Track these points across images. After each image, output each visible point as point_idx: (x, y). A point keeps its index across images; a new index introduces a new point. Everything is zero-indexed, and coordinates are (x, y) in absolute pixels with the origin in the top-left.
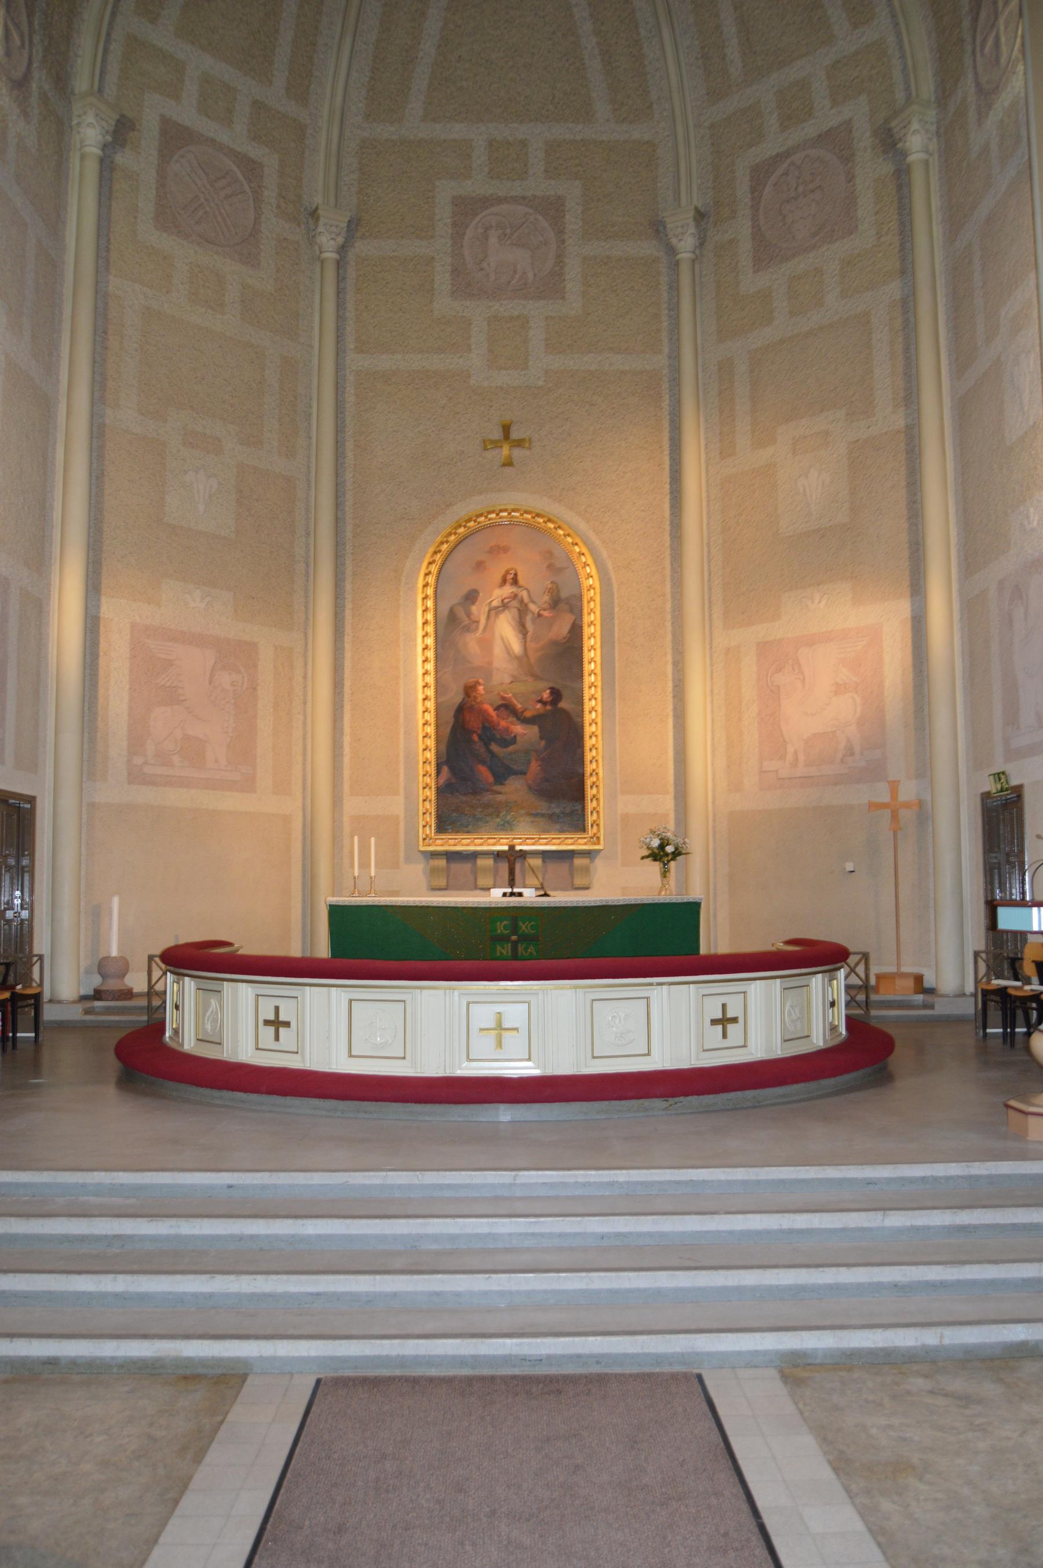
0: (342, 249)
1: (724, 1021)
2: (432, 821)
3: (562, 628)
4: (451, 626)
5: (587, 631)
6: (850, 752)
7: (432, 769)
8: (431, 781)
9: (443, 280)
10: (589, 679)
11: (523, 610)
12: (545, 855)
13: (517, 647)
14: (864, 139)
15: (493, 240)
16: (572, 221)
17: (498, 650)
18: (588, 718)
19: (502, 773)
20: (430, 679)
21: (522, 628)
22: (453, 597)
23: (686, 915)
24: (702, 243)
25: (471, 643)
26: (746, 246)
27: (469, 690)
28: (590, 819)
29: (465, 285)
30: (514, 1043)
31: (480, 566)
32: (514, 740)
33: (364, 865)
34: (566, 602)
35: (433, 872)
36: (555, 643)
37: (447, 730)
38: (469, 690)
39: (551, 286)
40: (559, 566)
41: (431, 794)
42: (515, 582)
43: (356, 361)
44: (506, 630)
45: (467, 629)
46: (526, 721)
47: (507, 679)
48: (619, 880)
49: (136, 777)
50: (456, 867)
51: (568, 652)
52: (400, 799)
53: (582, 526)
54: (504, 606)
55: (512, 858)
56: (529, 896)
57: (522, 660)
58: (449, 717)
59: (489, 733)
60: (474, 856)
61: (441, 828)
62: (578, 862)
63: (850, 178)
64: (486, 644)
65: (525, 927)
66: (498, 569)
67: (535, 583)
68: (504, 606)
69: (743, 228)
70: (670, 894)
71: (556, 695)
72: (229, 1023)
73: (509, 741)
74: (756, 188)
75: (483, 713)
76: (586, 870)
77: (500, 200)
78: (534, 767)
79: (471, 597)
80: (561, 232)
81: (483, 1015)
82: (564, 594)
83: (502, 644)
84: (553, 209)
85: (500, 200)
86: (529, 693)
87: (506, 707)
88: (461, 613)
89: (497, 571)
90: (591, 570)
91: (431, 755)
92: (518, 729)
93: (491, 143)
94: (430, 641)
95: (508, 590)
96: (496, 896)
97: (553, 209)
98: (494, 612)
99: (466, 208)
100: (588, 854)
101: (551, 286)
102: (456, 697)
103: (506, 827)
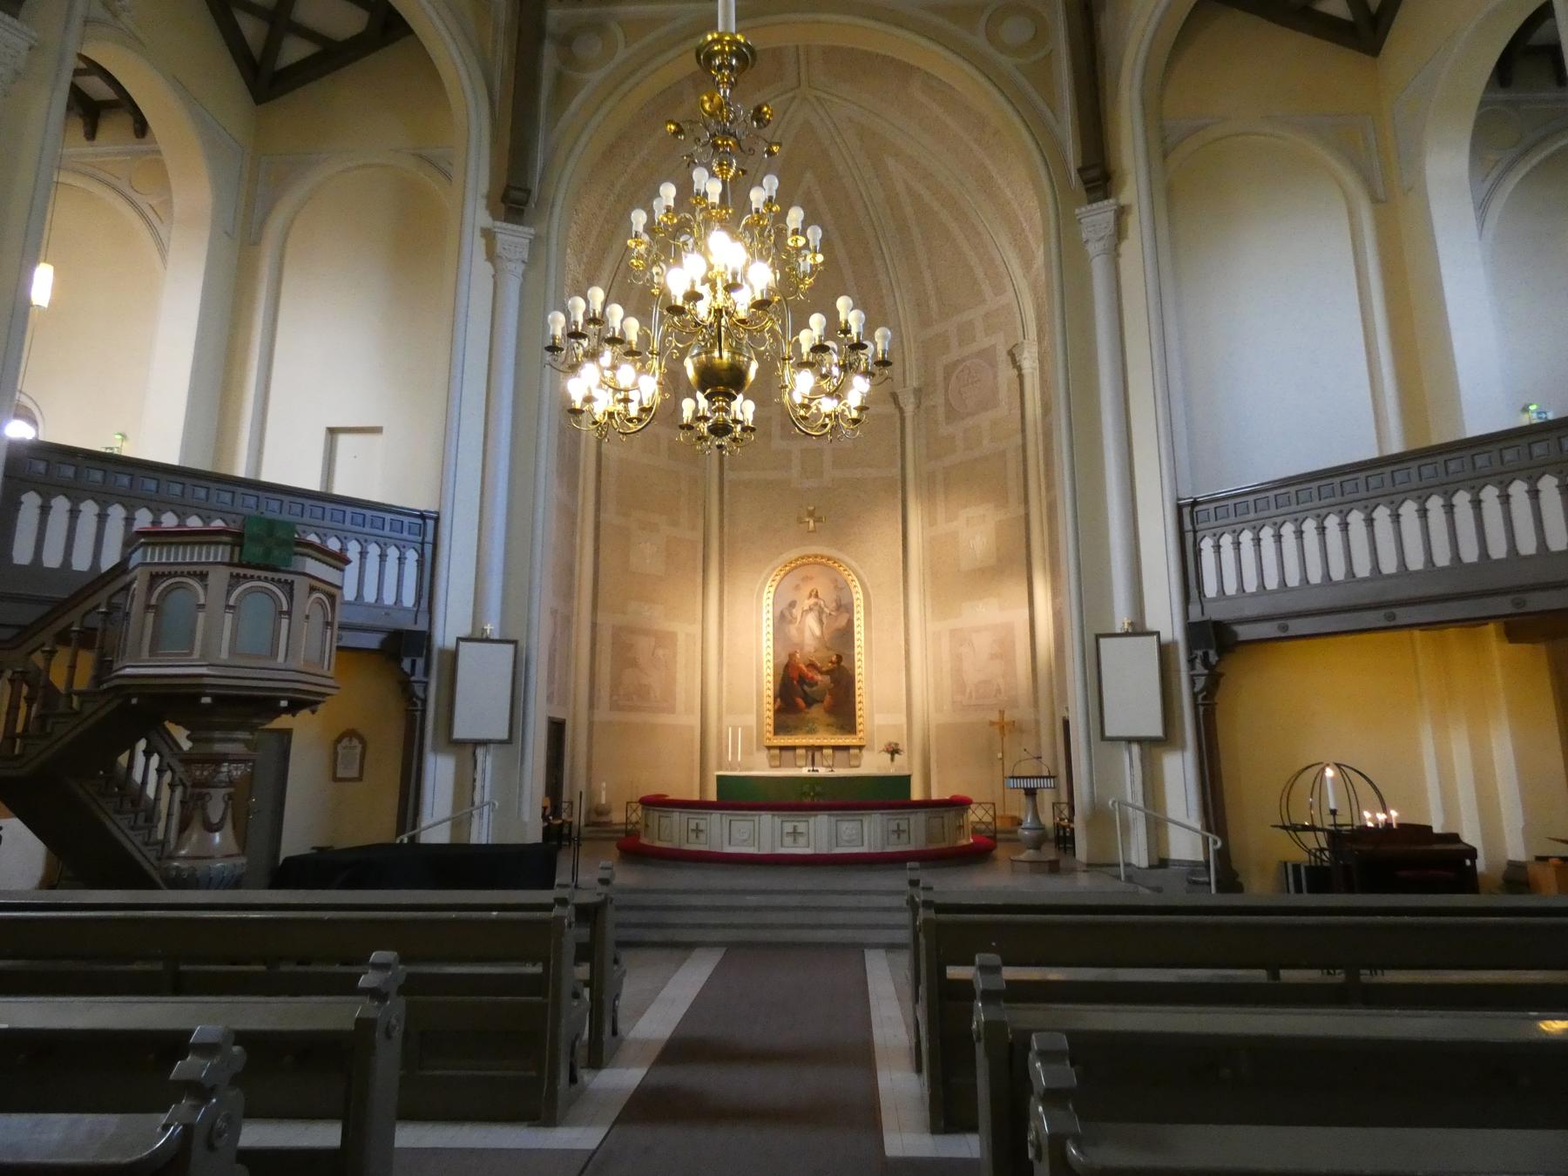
1: (898, 832)
2: (771, 729)
3: (842, 622)
6: (999, 691)
7: (771, 700)
8: (771, 707)
10: (857, 650)
11: (821, 612)
12: (835, 748)
13: (817, 632)
14: (1002, 356)
17: (807, 634)
18: (857, 671)
19: (809, 704)
21: (821, 621)
22: (783, 604)
24: (918, 407)
25: (793, 630)
26: (941, 410)
27: (792, 656)
28: (859, 728)
30: (802, 840)
31: (797, 587)
33: (735, 753)
34: (844, 607)
35: (772, 758)
36: (838, 630)
40: (841, 588)
41: (771, 714)
43: (729, 475)
46: (822, 673)
48: (873, 764)
49: (615, 706)
50: (788, 755)
51: (846, 634)
52: (754, 716)
53: (854, 564)
54: (811, 609)
55: (814, 749)
56: (823, 772)
57: (821, 639)
58: (781, 671)
59: (803, 679)
60: (794, 748)
61: (776, 733)
62: (852, 751)
63: (995, 377)
64: (801, 631)
65: (818, 789)
66: (806, 590)
67: (827, 597)
68: (811, 609)
69: (939, 399)
70: (892, 770)
71: (839, 658)
72: (675, 831)
73: (813, 683)
74: (947, 378)
75: (800, 670)
76: (858, 757)
78: (828, 697)
79: (792, 605)
81: (788, 827)
83: (810, 631)
86: (824, 658)
87: (811, 665)
89: (806, 590)
90: (859, 589)
91: (771, 693)
92: (819, 677)
95: (813, 600)
96: (804, 771)
98: (805, 612)
100: (860, 748)
102: (784, 660)
103: (812, 731)
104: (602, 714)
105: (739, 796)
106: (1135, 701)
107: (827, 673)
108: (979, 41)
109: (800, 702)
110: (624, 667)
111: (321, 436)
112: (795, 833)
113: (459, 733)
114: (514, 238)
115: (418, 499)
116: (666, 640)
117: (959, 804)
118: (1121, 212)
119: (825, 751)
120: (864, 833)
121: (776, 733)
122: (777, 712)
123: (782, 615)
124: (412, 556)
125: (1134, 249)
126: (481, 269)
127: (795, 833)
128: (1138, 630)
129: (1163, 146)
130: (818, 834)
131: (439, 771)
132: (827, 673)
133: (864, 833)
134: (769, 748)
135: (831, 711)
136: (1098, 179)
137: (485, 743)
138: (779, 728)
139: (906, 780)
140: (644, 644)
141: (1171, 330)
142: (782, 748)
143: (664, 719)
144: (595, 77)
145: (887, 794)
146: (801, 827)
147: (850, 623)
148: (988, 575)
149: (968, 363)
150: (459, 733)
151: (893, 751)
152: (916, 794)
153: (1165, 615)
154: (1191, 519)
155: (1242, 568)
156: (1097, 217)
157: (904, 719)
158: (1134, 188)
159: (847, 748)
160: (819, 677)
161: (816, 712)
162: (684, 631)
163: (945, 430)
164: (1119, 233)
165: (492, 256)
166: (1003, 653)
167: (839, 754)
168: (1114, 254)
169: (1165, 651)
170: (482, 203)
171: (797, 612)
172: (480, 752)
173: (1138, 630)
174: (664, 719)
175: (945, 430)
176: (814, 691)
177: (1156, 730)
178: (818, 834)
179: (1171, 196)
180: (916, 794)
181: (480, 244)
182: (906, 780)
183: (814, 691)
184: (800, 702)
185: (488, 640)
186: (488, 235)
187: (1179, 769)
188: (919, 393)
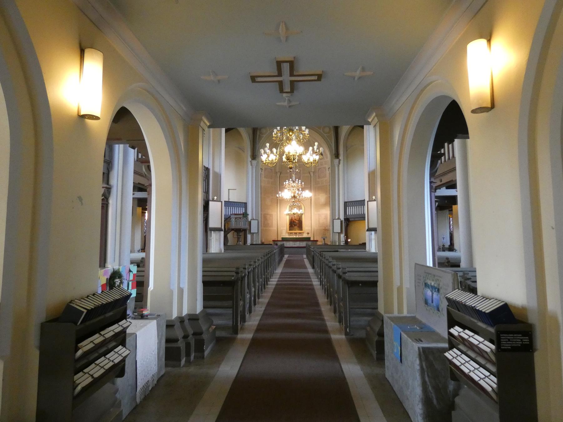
48: (305, 235)
105: (284, 239)
106: (337, 228)
108: (321, 131)
110: (265, 221)
114: (254, 162)
116: (271, 215)
117: (317, 241)
118: (340, 160)
120: (303, 244)
122: (290, 227)
125: (341, 165)
126: (250, 167)
128: (339, 219)
129: (346, 148)
130: (298, 244)
131: (249, 237)
133: (303, 244)
136: (337, 155)
138: (290, 230)
139: (310, 238)
140: (268, 216)
141: (346, 178)
143: (271, 228)
144: (265, 136)
145: (308, 239)
148: (325, 205)
151: (308, 234)
152: (312, 239)
153: (342, 217)
154: (346, 204)
155: (352, 211)
156: (336, 161)
158: (341, 157)
161: (296, 227)
162: (274, 214)
163: (318, 180)
164: (339, 163)
165: (251, 165)
166: (326, 218)
168: (339, 166)
169: (341, 222)
173: (339, 219)
174: (271, 228)
175: (318, 180)
176: (296, 223)
177: (340, 231)
178: (298, 244)
179: (347, 157)
180: (312, 239)
182: (310, 238)
183: (296, 223)
187: (342, 236)
188: (314, 172)
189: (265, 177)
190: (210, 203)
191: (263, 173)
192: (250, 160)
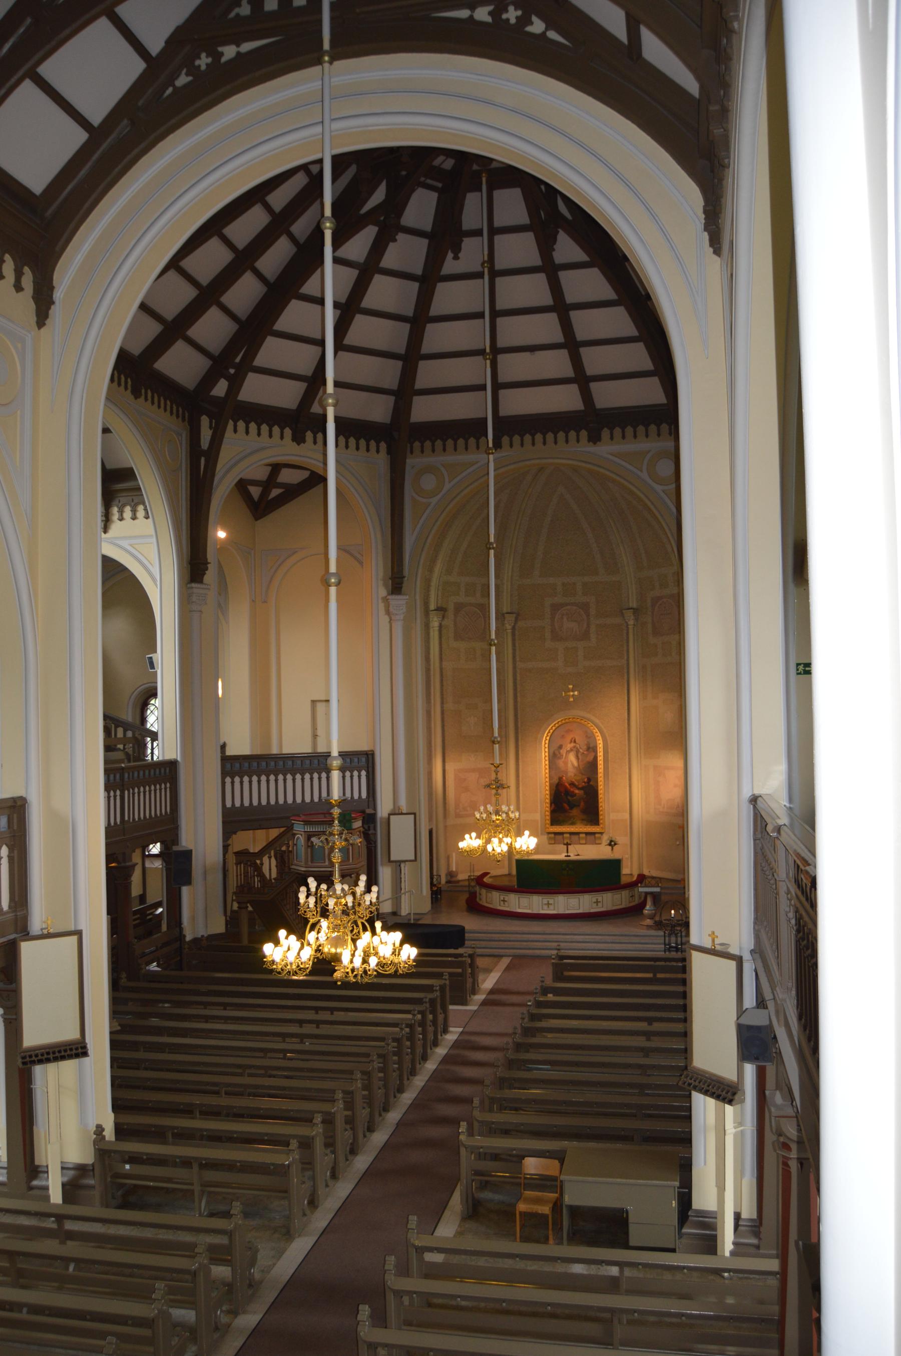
0: (513, 628)
1: (597, 902)
3: (590, 758)
4: (554, 757)
5: (599, 759)
6: (678, 807)
9: (548, 635)
11: (578, 752)
12: (587, 834)
13: (576, 764)
15: (565, 619)
16: (593, 611)
17: (570, 765)
19: (571, 808)
20: (547, 775)
21: (577, 758)
23: (616, 864)
27: (560, 779)
28: (601, 822)
29: (556, 637)
31: (563, 736)
32: (575, 795)
35: (550, 839)
36: (589, 763)
37: (553, 792)
38: (560, 779)
39: (585, 636)
40: (590, 737)
42: (575, 742)
43: (520, 665)
44: (572, 758)
45: (559, 758)
46: (579, 789)
47: (573, 775)
49: (458, 816)
51: (593, 765)
53: (597, 721)
54: (571, 750)
57: (578, 768)
59: (567, 793)
61: (552, 824)
62: (597, 835)
64: (566, 763)
66: (569, 737)
67: (581, 743)
68: (571, 750)
71: (589, 780)
72: (495, 900)
76: (600, 838)
77: (567, 604)
78: (582, 804)
79: (561, 747)
80: (588, 616)
81: (545, 901)
82: (591, 746)
83: (571, 763)
84: (585, 607)
85: (567, 604)
88: (557, 752)
91: (548, 801)
92: (577, 791)
93: (563, 584)
94: (547, 762)
95: (573, 745)
97: (585, 607)
98: (568, 752)
99: (555, 608)
101: (585, 636)
102: (556, 781)
103: (573, 824)
104: (451, 821)
107: (582, 788)
109: (565, 805)
111: (310, 703)
112: (548, 904)
113: (392, 859)
115: (365, 747)
119: (581, 835)
121: (552, 824)
123: (554, 754)
124: (364, 773)
127: (548, 904)
132: (582, 788)
134: (549, 833)
135: (584, 812)
137: (405, 861)
138: (554, 821)
139: (616, 864)
142: (556, 834)
146: (551, 901)
147: (596, 758)
149: (665, 600)
150: (392, 859)
157: (627, 816)
159: (594, 833)
160: (577, 791)
161: (575, 812)
165: (388, 612)
167: (589, 837)
170: (381, 583)
171: (563, 751)
172: (402, 865)
181: (382, 606)
184: (565, 805)
185: (402, 814)
186: (385, 600)
189: (458, 637)
190: (27, 949)
191: (449, 622)
192: (383, 592)
